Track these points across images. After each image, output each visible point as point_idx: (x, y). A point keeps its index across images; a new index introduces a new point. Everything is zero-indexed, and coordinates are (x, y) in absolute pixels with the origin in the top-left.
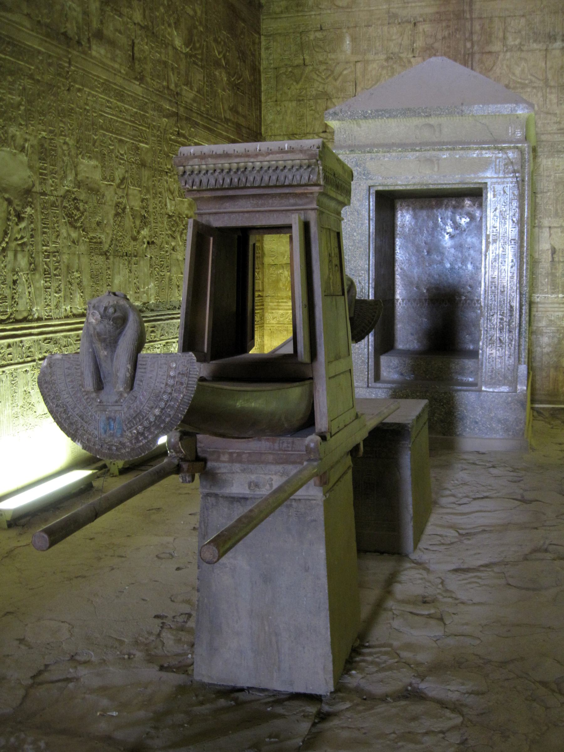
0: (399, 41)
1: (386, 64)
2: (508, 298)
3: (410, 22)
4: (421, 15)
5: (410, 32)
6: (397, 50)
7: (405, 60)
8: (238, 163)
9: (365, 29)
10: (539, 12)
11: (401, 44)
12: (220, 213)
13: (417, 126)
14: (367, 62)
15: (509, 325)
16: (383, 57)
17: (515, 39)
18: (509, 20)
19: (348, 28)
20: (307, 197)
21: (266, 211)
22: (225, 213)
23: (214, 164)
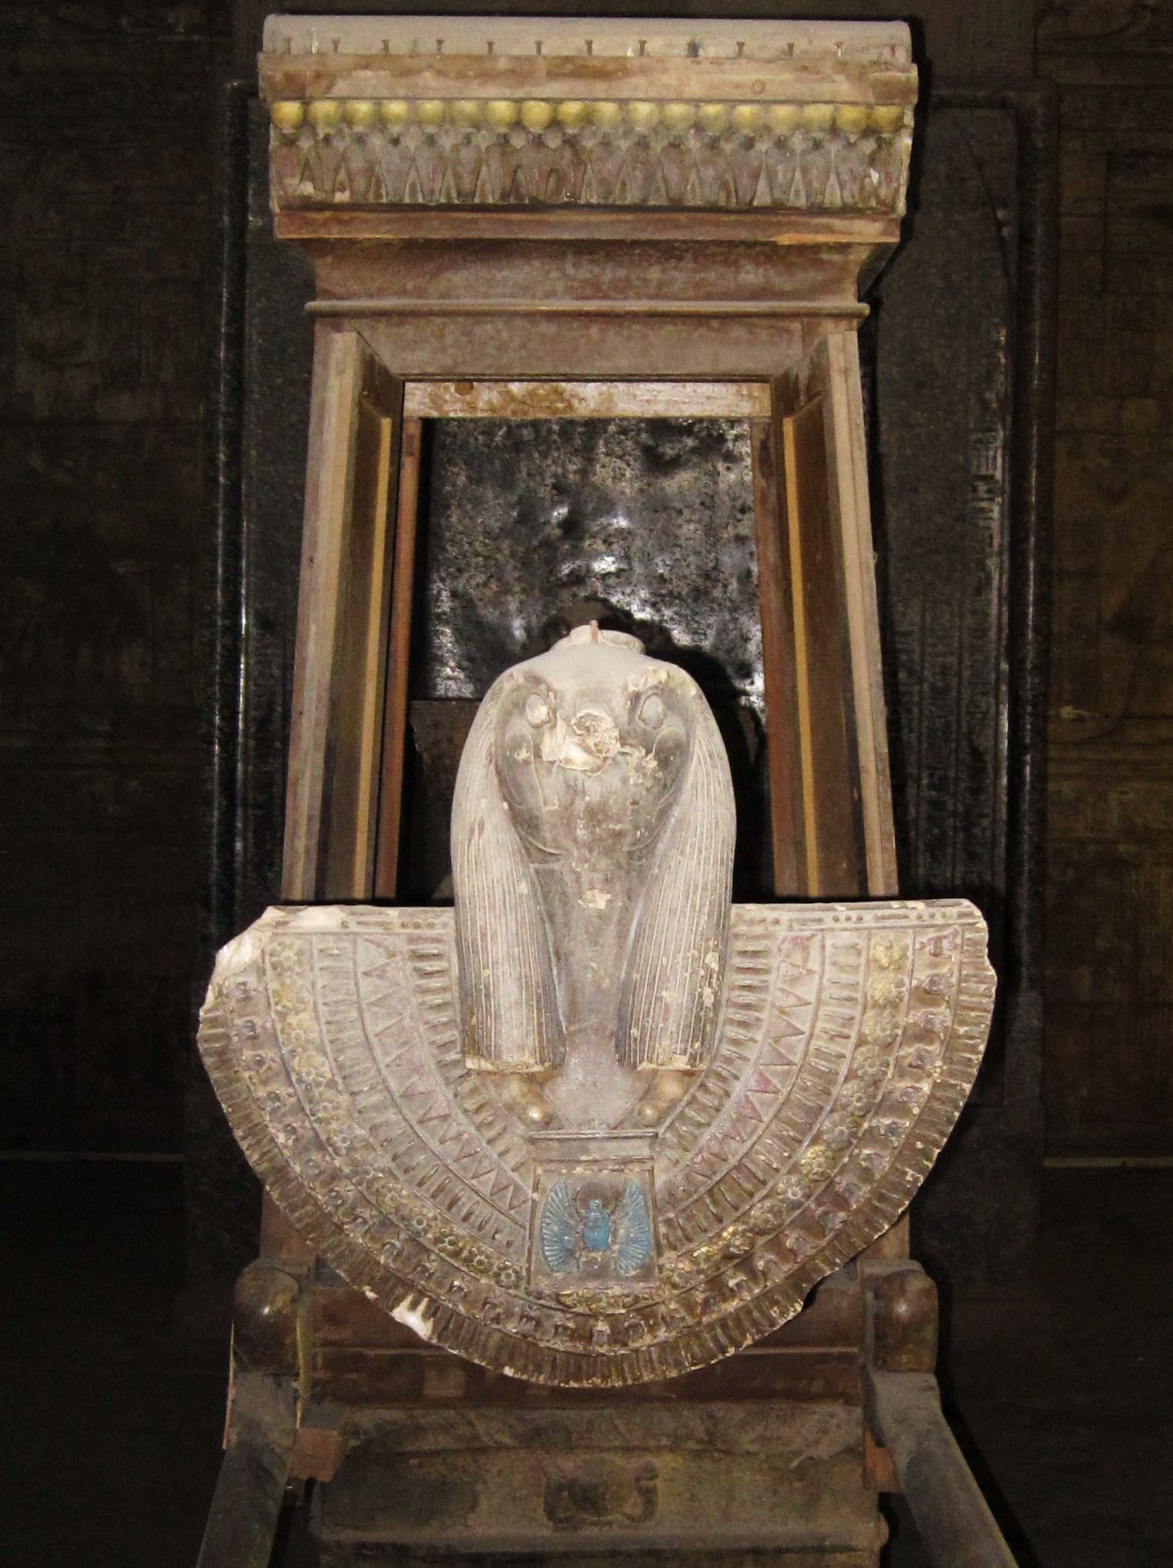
2: (964, 719)
8: (555, 102)
12: (431, 314)
15: (967, 830)
20: (819, 264)
21: (634, 316)
22: (446, 314)
23: (448, 101)
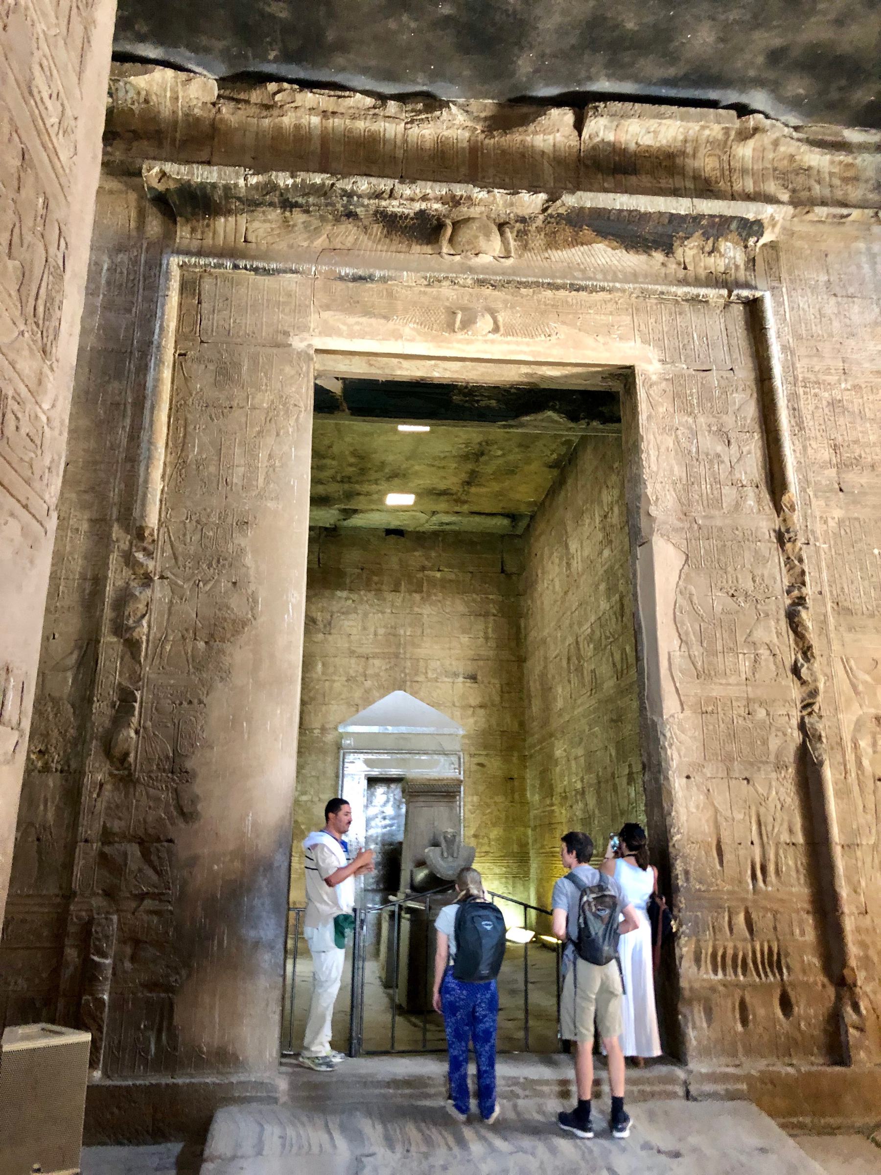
14: (334, 681)
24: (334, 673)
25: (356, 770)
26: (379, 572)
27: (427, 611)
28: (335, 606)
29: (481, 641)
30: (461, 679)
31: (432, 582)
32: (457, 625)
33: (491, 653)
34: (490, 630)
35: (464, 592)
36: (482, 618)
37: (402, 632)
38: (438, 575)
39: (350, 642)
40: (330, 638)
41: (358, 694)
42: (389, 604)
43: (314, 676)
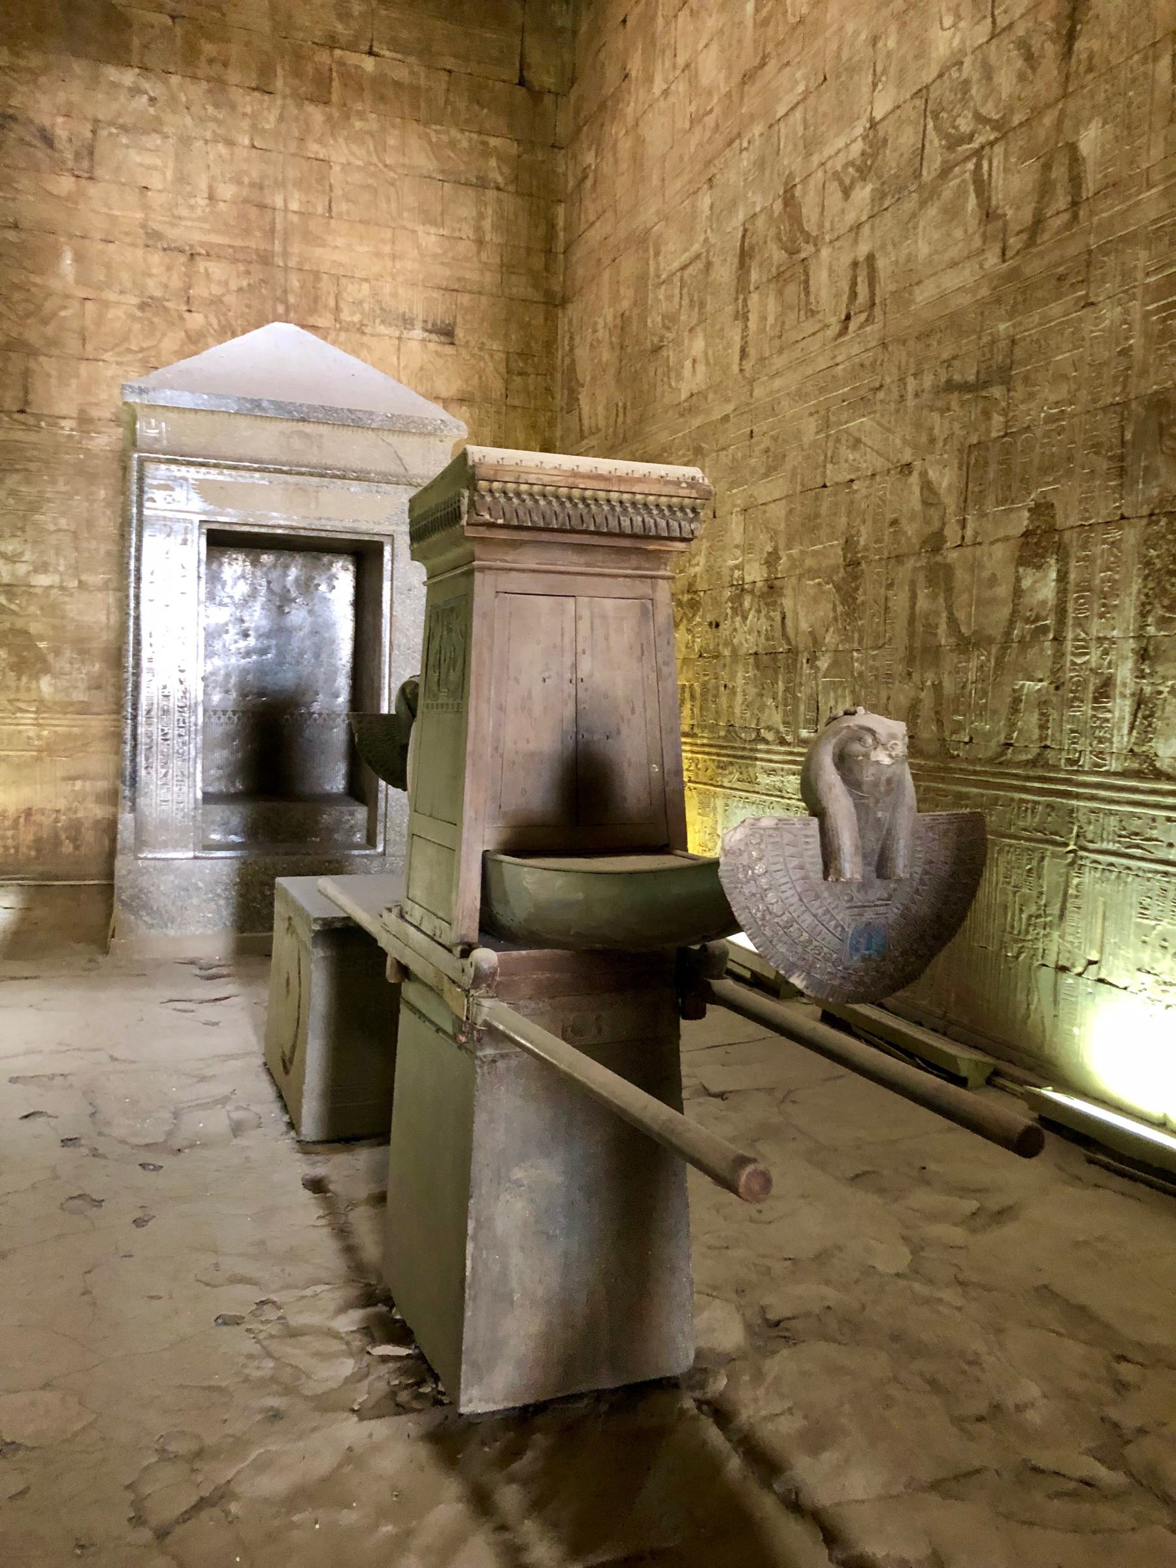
0: (164, 279)
1: (139, 314)
3: (182, 251)
4: (202, 244)
5: (183, 269)
6: (158, 293)
7: (175, 314)
9: (101, 246)
10: (389, 279)
11: (166, 286)
13: (282, 433)
16: (135, 301)
17: (353, 314)
18: (343, 281)
19: (71, 236)
24: (108, 284)
25: (178, 505)
26: (219, 32)
27: (342, 153)
28: (103, 107)
29: (465, 247)
30: (418, 333)
31: (354, 82)
32: (411, 201)
33: (489, 279)
34: (487, 224)
35: (426, 124)
36: (471, 192)
37: (279, 202)
38: (369, 64)
39: (145, 207)
40: (93, 190)
41: (170, 342)
42: (245, 124)
43: (55, 284)
